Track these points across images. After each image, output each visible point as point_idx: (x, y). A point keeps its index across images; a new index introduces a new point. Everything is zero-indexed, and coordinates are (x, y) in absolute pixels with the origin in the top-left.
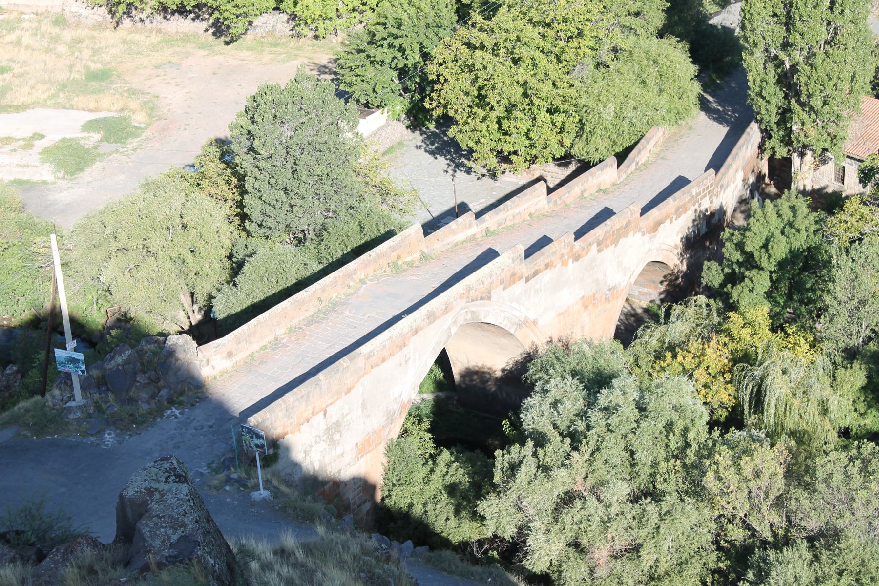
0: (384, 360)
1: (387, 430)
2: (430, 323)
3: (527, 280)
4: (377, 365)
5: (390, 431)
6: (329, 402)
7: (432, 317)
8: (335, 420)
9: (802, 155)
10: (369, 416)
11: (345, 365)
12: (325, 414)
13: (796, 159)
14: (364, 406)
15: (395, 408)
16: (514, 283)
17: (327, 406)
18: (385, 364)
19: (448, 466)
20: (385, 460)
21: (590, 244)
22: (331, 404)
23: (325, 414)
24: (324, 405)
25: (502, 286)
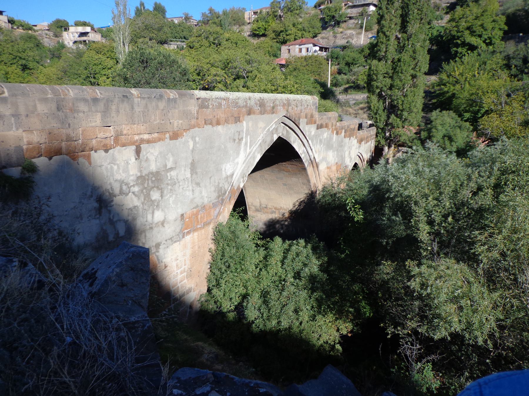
0: (218, 123)
1: (218, 210)
2: (262, 113)
3: (317, 129)
4: (211, 124)
5: (219, 214)
6: (146, 137)
7: (263, 108)
8: (153, 168)
9: (389, 147)
10: (198, 184)
11: (172, 96)
12: (138, 152)
13: (386, 148)
14: (193, 167)
15: (226, 187)
16: (312, 124)
17: (142, 141)
18: (220, 128)
19: (287, 251)
20: (213, 247)
21: (342, 129)
22: (148, 142)
23: (138, 152)
24: (136, 138)
25: (306, 120)
